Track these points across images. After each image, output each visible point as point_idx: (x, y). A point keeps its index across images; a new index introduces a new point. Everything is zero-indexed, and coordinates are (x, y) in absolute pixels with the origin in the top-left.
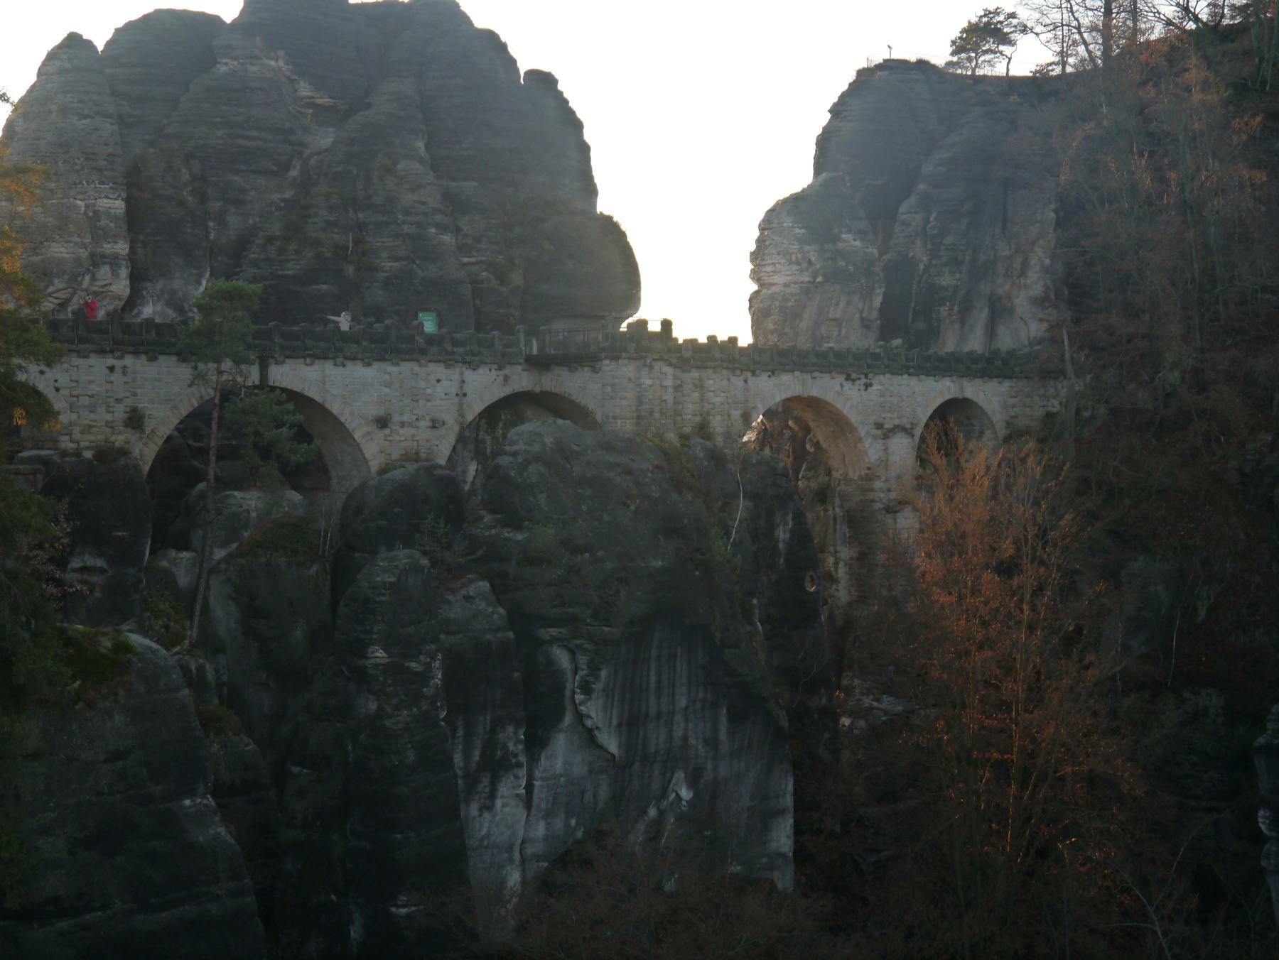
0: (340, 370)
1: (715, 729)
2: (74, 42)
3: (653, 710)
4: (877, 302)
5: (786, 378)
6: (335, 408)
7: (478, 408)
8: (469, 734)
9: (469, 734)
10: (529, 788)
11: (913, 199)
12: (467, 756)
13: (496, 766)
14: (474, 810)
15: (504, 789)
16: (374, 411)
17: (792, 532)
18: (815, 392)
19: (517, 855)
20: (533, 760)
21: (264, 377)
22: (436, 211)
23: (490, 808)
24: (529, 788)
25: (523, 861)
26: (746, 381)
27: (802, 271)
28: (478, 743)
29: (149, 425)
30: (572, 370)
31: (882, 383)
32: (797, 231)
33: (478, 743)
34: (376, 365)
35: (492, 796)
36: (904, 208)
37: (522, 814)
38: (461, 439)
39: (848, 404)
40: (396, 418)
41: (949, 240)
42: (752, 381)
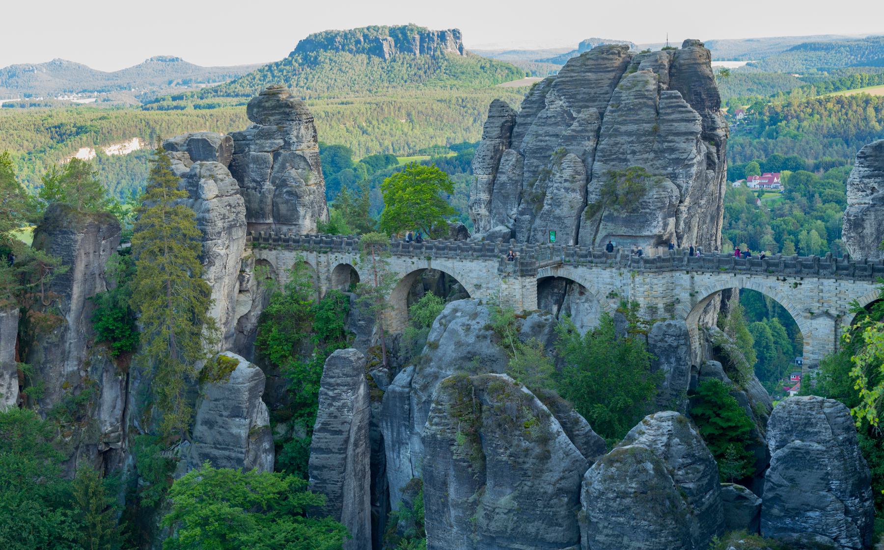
0: (461, 263)
5: (724, 277)
8: (392, 426)
12: (392, 435)
17: (676, 369)
18: (748, 286)
21: (429, 265)
22: (566, 181)
26: (693, 278)
27: (867, 195)
28: (395, 430)
30: (575, 267)
31: (809, 284)
32: (861, 169)
33: (395, 430)
34: (476, 261)
39: (779, 296)
40: (484, 286)
42: (698, 278)
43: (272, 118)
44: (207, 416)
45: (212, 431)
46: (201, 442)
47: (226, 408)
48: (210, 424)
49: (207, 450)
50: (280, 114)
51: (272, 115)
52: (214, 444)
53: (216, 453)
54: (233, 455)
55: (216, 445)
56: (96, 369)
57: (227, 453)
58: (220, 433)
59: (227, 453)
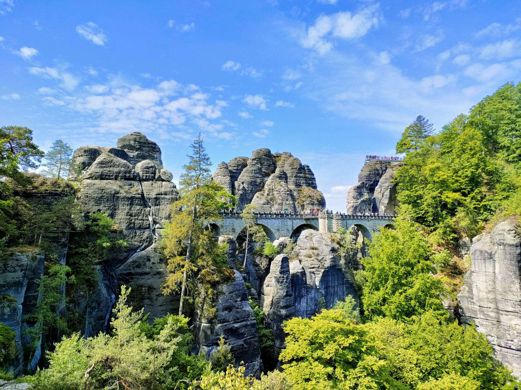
1: (343, 289)
2: (224, 163)
3: (331, 285)
4: (372, 206)
6: (269, 227)
7: (296, 227)
8: (295, 290)
9: (295, 290)
10: (307, 300)
11: (378, 186)
13: (301, 297)
14: (297, 305)
15: (302, 300)
16: (276, 228)
19: (305, 314)
20: (307, 294)
23: (300, 304)
24: (307, 300)
25: (306, 314)
29: (236, 231)
35: (300, 302)
36: (376, 188)
37: (306, 305)
38: (293, 233)
41: (385, 194)
43: (144, 149)
44: (227, 304)
45: (231, 313)
46: (225, 322)
47: (238, 296)
48: (229, 309)
49: (231, 326)
50: (149, 147)
51: (144, 147)
52: (234, 320)
53: (236, 325)
54: (249, 323)
55: (236, 321)
56: (79, 304)
57: (244, 323)
58: (237, 312)
59: (244, 323)
